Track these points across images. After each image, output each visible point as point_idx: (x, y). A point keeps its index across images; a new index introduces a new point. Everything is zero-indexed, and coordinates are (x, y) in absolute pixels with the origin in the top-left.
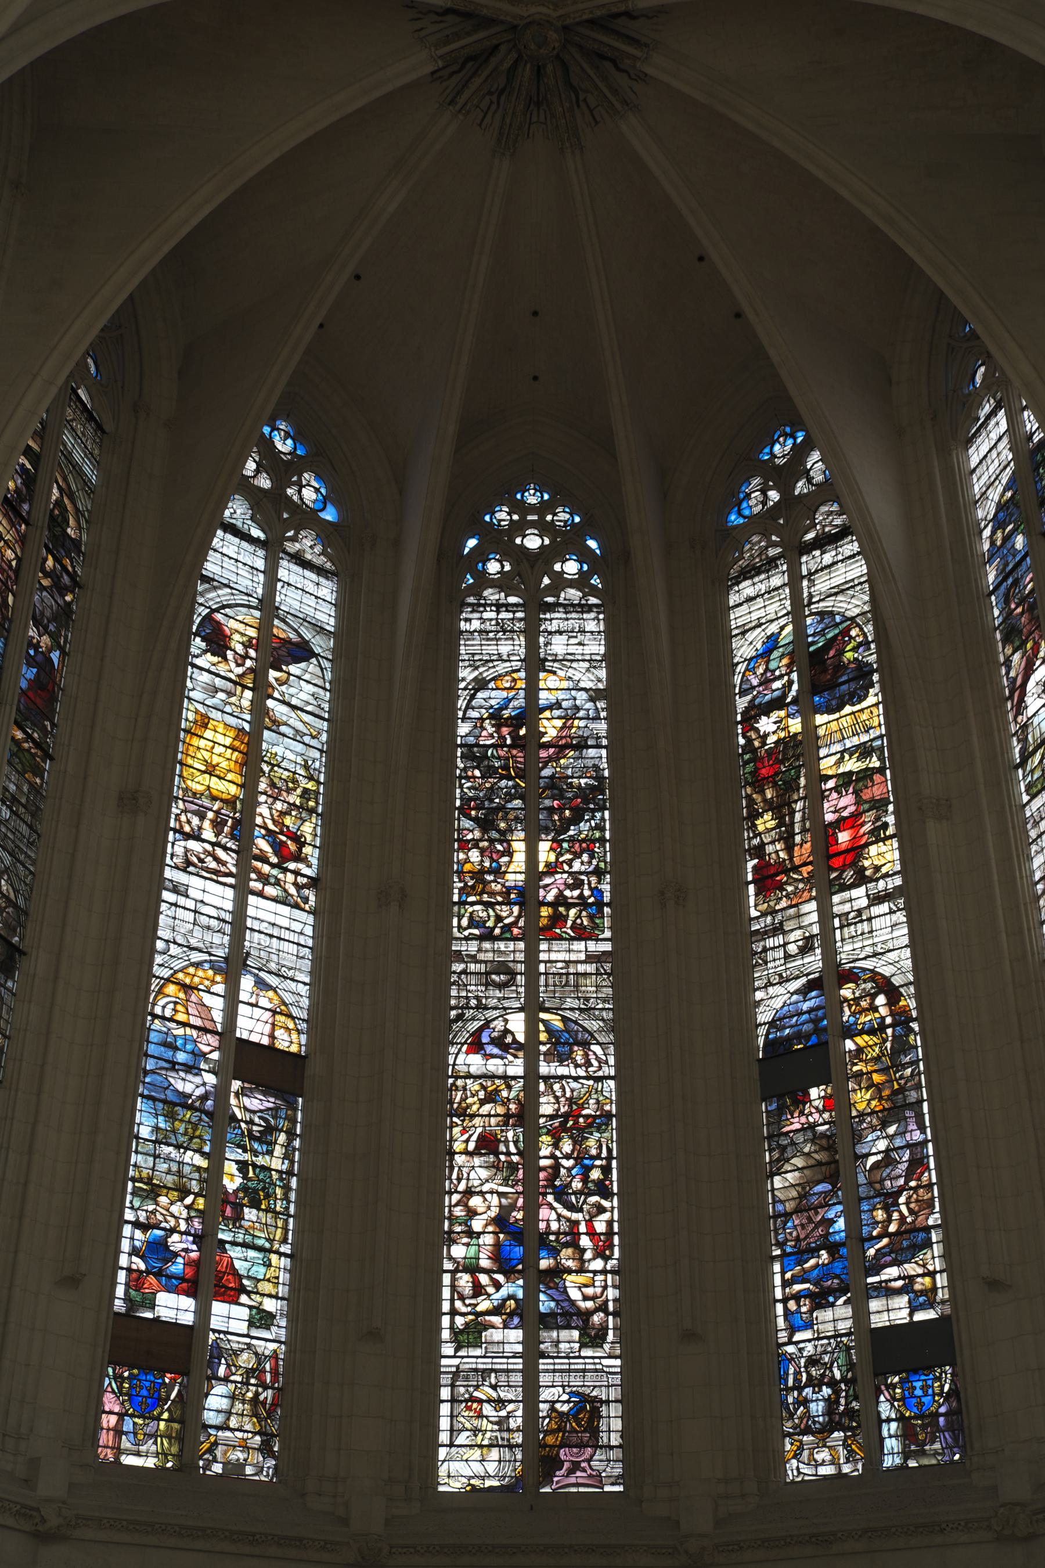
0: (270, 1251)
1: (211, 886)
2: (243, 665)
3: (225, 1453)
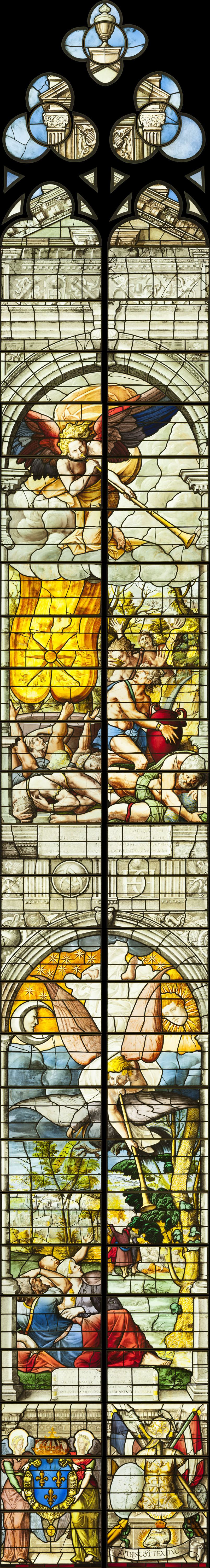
0: (180, 1295)
1: (67, 832)
2: (82, 474)
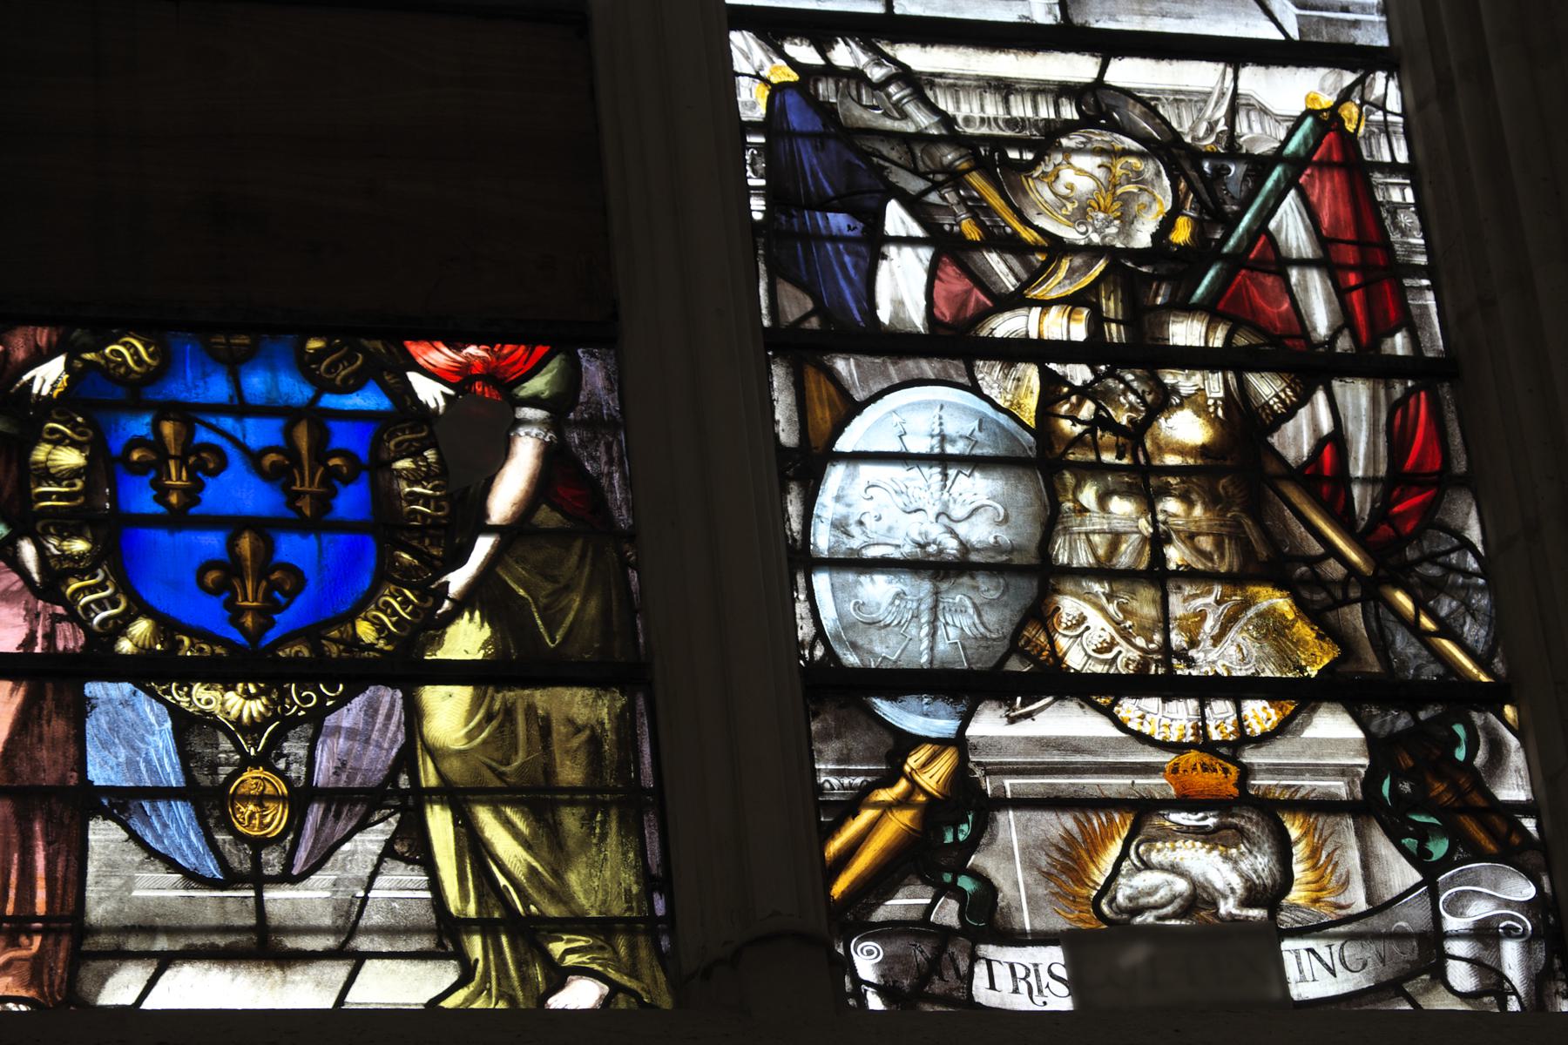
3: (1068, 864)
